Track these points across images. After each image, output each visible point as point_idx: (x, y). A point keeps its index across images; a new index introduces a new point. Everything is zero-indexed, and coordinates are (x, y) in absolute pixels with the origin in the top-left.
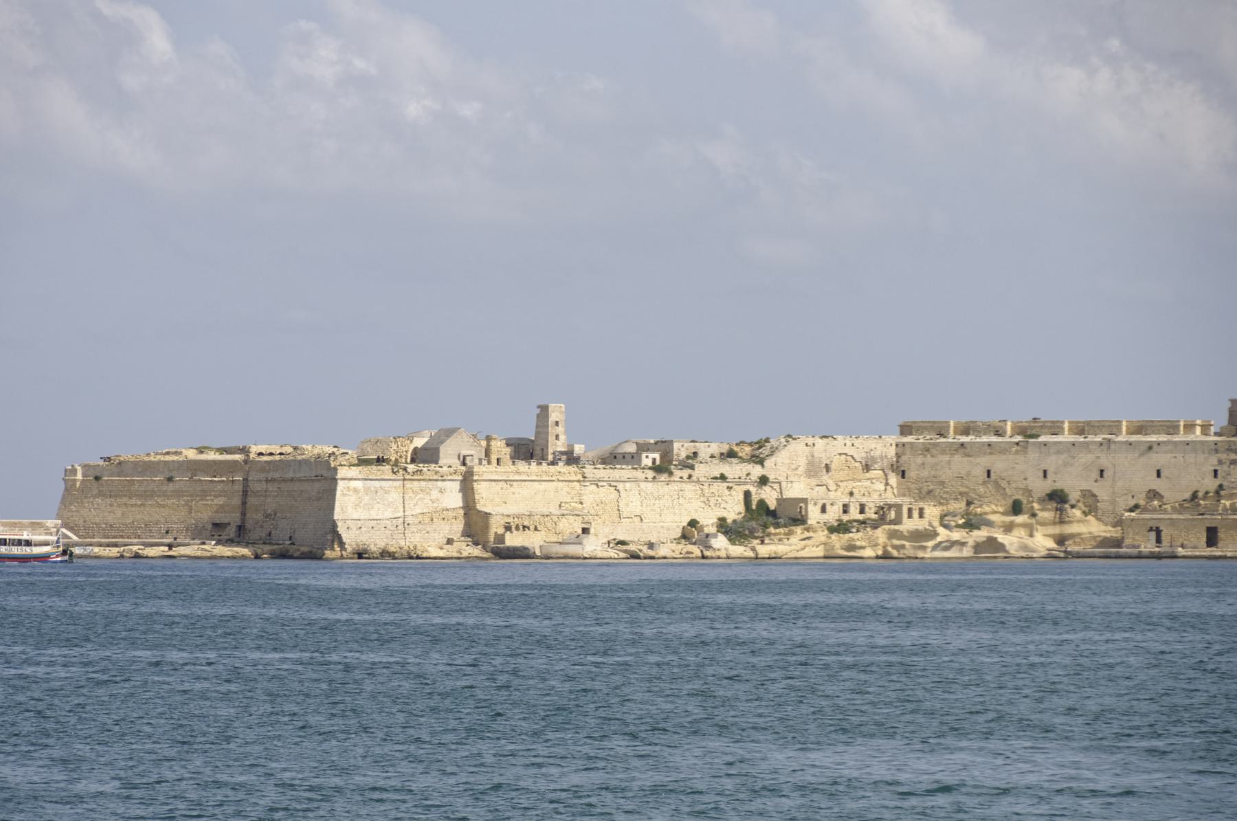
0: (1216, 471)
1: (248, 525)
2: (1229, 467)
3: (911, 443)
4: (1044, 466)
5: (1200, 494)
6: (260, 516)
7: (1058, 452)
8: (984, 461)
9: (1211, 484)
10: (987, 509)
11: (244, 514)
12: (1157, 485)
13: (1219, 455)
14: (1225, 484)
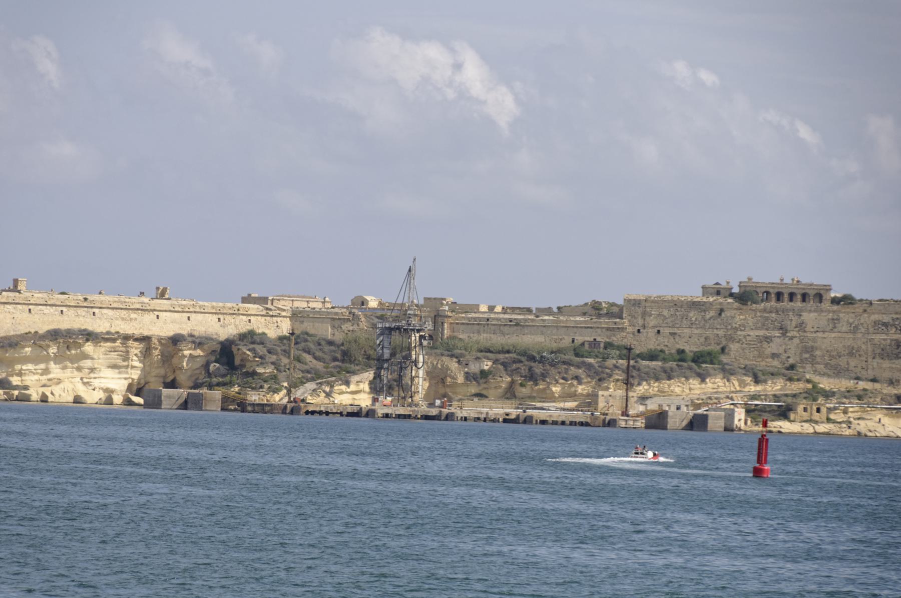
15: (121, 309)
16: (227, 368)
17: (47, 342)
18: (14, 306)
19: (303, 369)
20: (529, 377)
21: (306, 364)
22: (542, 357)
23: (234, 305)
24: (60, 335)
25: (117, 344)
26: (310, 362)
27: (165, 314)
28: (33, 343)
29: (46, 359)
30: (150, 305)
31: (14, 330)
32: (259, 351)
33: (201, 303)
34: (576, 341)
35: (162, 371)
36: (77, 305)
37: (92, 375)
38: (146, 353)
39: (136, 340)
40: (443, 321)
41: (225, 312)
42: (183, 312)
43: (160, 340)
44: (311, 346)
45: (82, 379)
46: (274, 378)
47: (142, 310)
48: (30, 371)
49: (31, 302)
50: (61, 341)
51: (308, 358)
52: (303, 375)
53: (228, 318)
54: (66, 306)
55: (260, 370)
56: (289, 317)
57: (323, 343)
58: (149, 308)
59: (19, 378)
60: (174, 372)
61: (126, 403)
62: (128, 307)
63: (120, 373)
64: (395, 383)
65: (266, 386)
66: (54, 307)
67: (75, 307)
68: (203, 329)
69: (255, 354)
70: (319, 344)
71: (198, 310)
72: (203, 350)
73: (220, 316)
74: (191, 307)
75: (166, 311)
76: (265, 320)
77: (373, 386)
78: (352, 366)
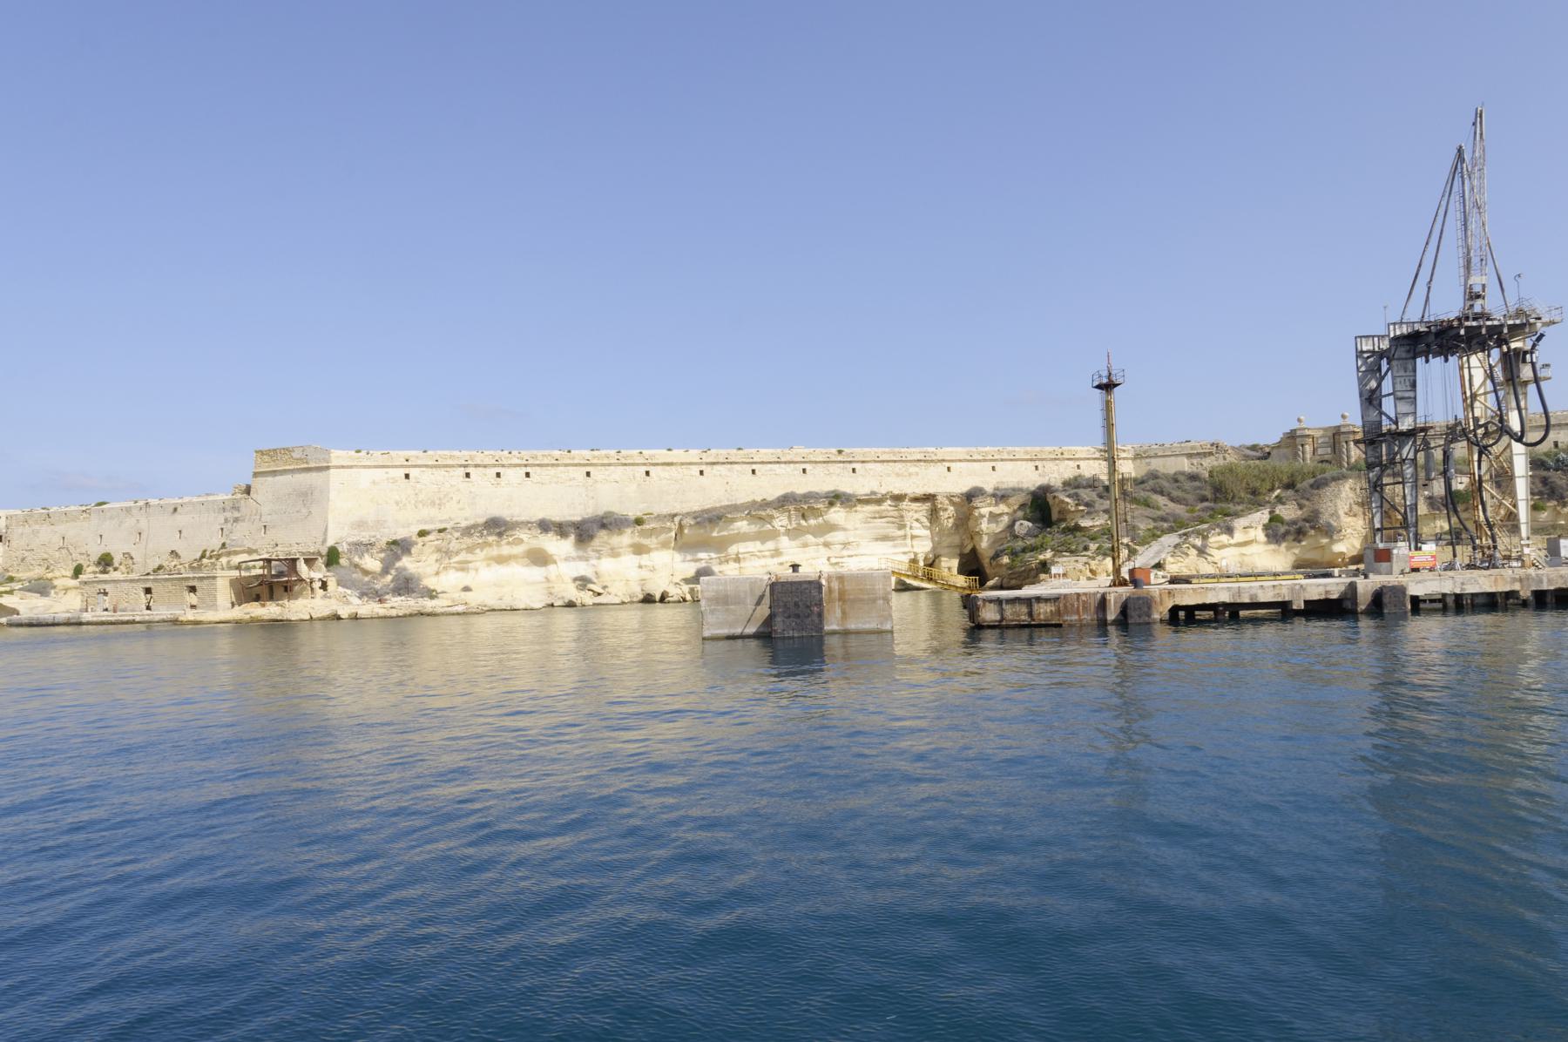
0: (222, 529)
2: (232, 525)
3: (16, 515)
4: (99, 533)
5: (208, 554)
7: (111, 518)
8: (61, 528)
9: (215, 543)
10: (57, 574)
13: (225, 514)
14: (228, 542)
15: (895, 461)
16: (1039, 525)
17: (769, 511)
18: (729, 466)
19: (1155, 516)
20: (1548, 494)
21: (1158, 508)
22: (1558, 460)
23: (1056, 448)
24: (791, 500)
25: (882, 508)
26: (1165, 505)
27: (959, 464)
28: (748, 514)
29: (773, 535)
30: (936, 455)
31: (728, 500)
32: (1085, 496)
33: (1010, 448)
34: (1560, 445)
35: (956, 540)
36: (828, 460)
37: (845, 553)
38: (934, 514)
39: (916, 500)
40: (1347, 439)
41: (1044, 457)
42: (985, 460)
43: (950, 497)
44: (1165, 484)
45: (829, 559)
46: (1107, 532)
47: (925, 461)
48: (753, 554)
49: (755, 460)
50: (791, 508)
51: (1161, 500)
52: (1155, 524)
53: (1049, 465)
54: (811, 462)
55: (1085, 523)
56: (1131, 459)
57: (1181, 478)
58: (934, 458)
59: (737, 565)
60: (972, 538)
61: (899, 587)
62: (904, 459)
63: (895, 546)
64: (1307, 525)
65: (1093, 546)
66: (792, 465)
67: (824, 462)
68: (1015, 480)
69: (1078, 500)
70: (1176, 481)
71: (1006, 457)
72: (1008, 506)
73: (1037, 463)
74: (995, 455)
75: (960, 461)
76: (1100, 464)
77: (1270, 531)
78: (1231, 505)
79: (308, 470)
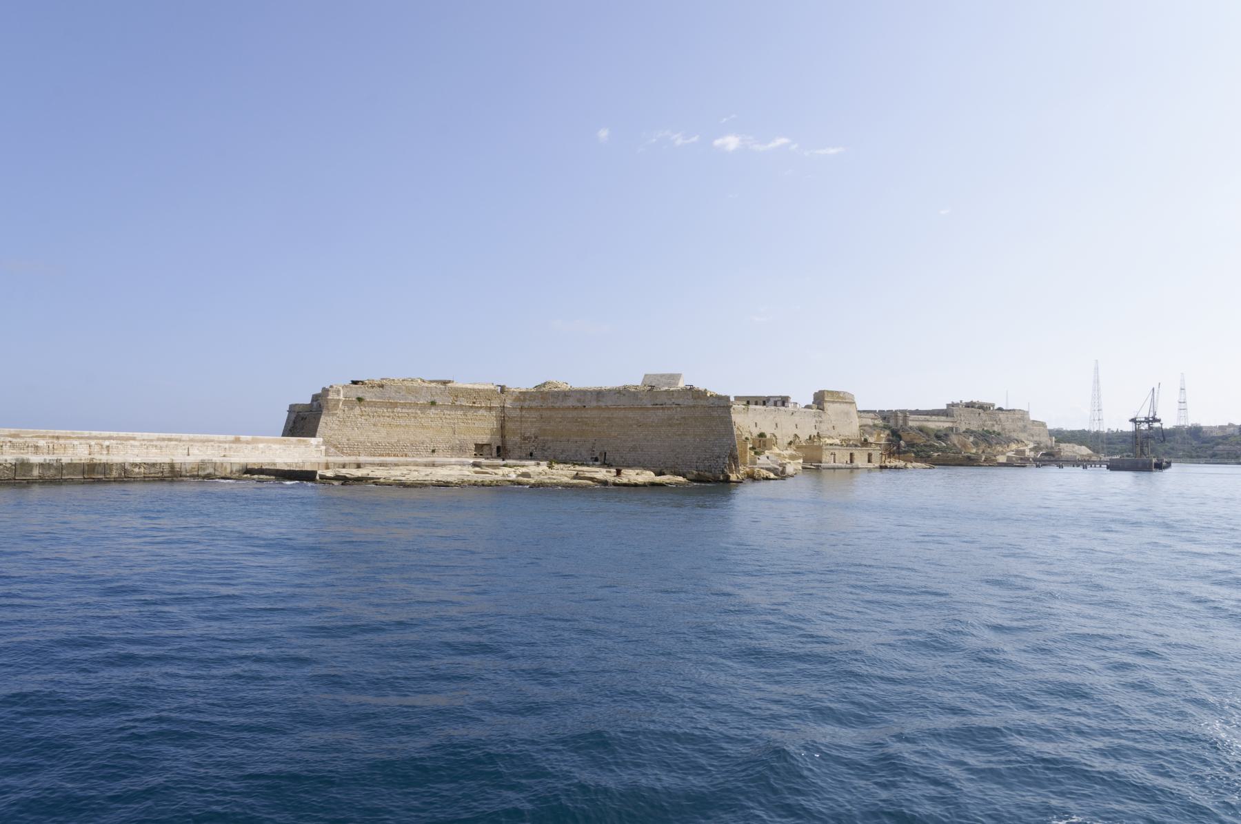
1: (509, 445)
5: (812, 436)
6: (517, 439)
7: (760, 414)
11: (503, 436)
12: (797, 432)
79: (846, 403)
